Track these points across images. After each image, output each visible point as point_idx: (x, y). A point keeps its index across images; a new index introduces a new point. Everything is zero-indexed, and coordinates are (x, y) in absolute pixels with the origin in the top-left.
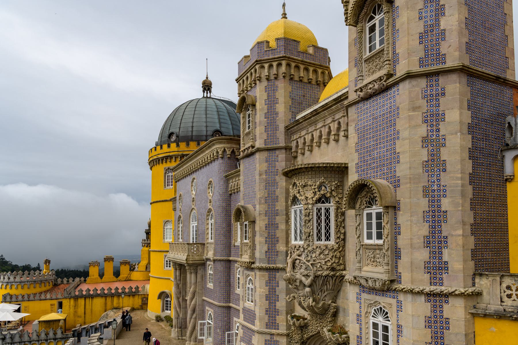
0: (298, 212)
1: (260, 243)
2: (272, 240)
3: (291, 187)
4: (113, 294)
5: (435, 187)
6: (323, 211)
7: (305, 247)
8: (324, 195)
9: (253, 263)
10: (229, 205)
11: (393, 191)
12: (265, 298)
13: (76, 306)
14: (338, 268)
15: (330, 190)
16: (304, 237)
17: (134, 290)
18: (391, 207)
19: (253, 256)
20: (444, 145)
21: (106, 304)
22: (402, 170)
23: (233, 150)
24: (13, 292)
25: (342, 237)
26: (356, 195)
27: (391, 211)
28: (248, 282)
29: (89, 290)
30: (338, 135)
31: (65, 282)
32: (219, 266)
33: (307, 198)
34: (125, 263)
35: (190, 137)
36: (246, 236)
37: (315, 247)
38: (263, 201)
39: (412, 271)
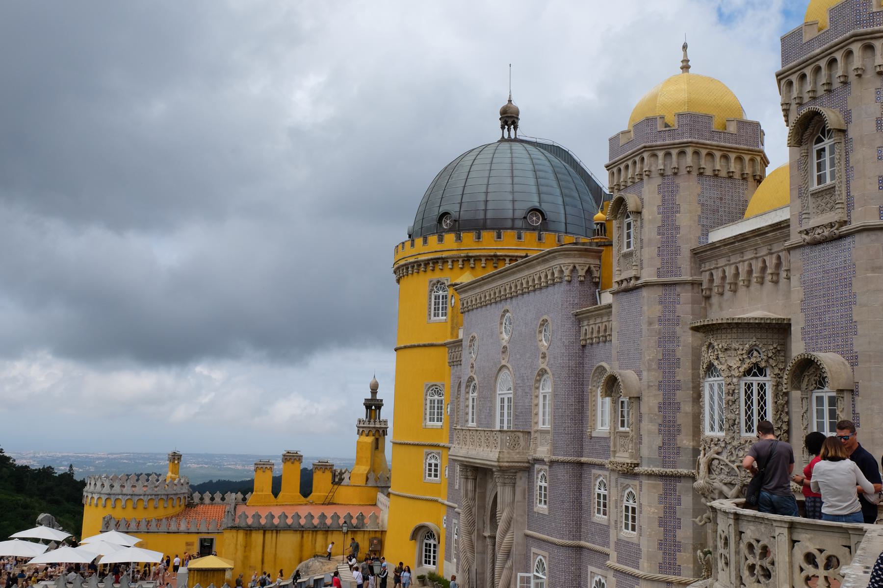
0: (716, 388)
2: (669, 429)
3: (704, 348)
4: (315, 527)
6: (755, 388)
7: (728, 441)
8: (756, 365)
9: (637, 465)
11: (849, 369)
12: (657, 523)
13: (247, 546)
15: (765, 358)
16: (726, 426)
17: (354, 522)
18: (847, 390)
19: (637, 453)
21: (301, 546)
23: (589, 268)
24: (119, 514)
25: (785, 427)
26: (802, 372)
27: (847, 395)
28: (625, 498)
29: (273, 517)
31: (207, 500)
32: (562, 473)
34: (324, 466)
37: (743, 442)
38: (654, 366)
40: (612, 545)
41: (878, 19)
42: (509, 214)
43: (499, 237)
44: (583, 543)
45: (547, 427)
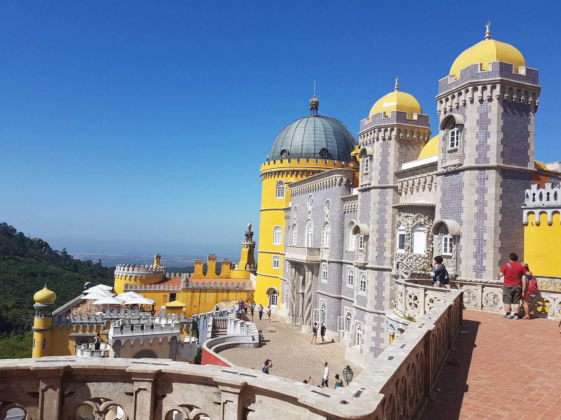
1: (372, 250)
2: (381, 249)
5: (481, 227)
7: (406, 255)
9: (367, 264)
10: (343, 220)
14: (428, 269)
20: (486, 206)
22: (464, 217)
26: (439, 227)
30: (431, 185)
33: (408, 224)
35: (300, 155)
36: (361, 245)
38: (376, 222)
39: (466, 270)
40: (355, 297)
41: (481, 76)
42: (313, 151)
43: (308, 161)
44: (342, 296)
45: (328, 246)
